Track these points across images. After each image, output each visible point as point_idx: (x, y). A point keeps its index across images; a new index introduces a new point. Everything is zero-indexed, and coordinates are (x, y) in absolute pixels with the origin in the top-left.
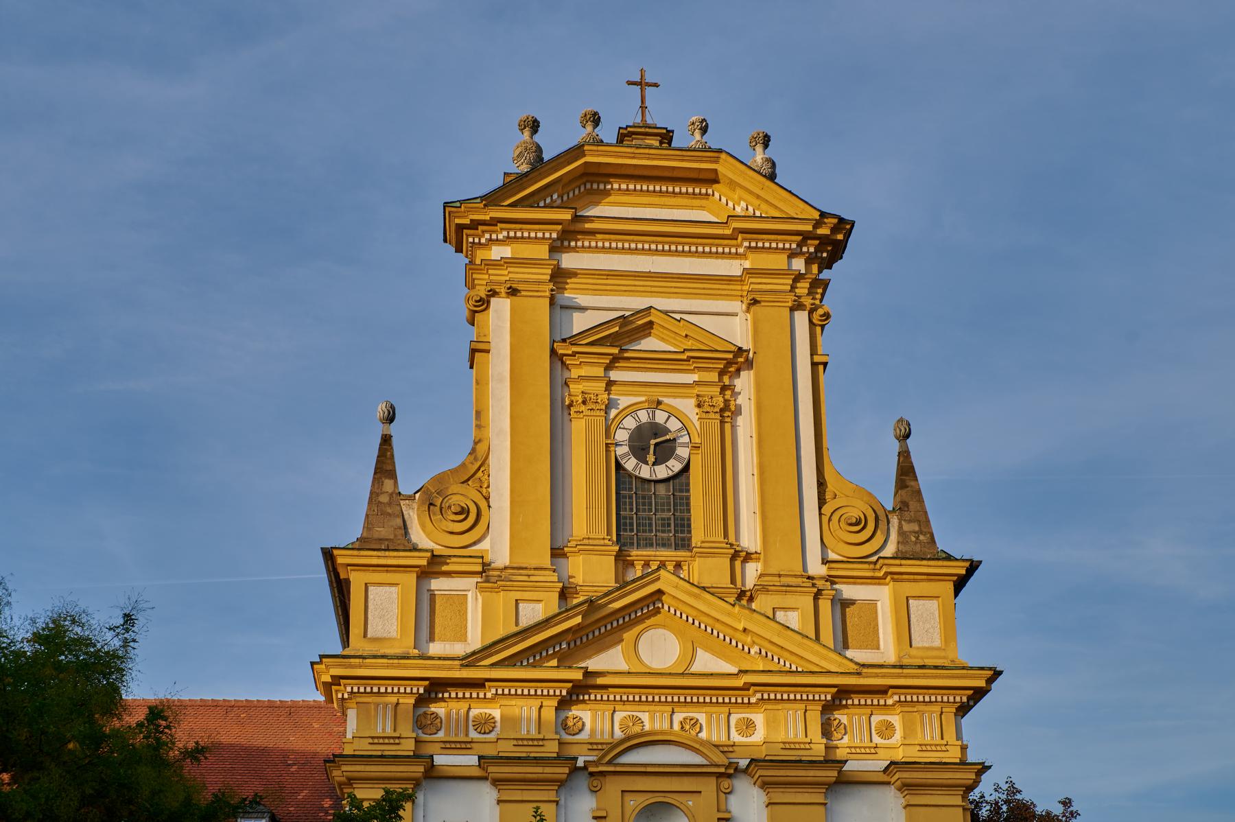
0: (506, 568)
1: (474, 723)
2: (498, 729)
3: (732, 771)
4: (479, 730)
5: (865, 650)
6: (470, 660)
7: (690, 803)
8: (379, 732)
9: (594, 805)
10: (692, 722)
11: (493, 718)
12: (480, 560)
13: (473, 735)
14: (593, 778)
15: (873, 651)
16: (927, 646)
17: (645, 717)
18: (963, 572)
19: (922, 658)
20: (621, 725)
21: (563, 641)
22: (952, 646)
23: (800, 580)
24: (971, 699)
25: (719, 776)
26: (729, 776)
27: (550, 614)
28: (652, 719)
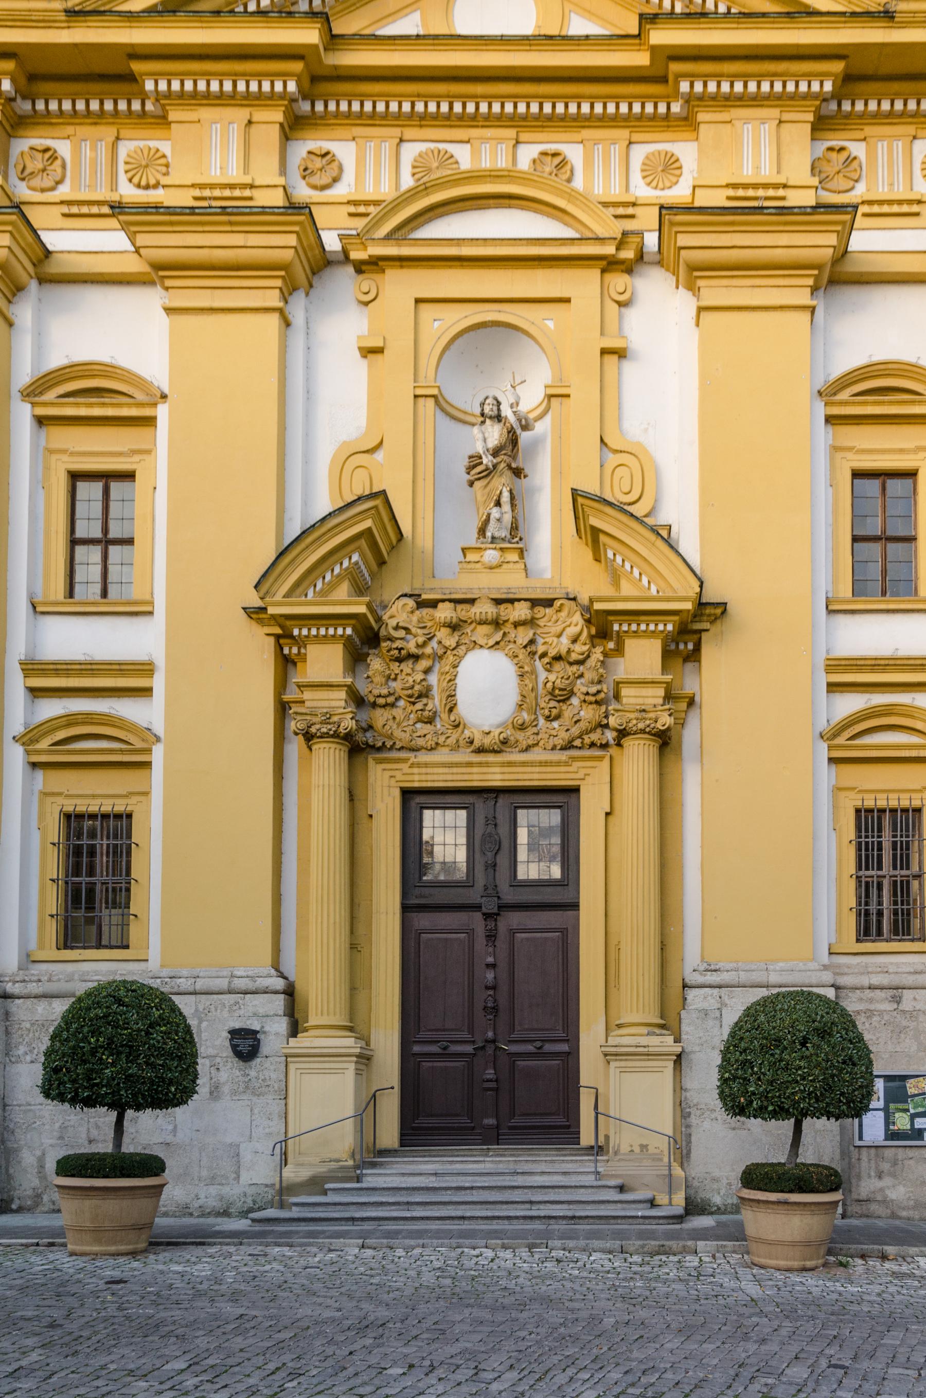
4: (136, 180)
10: (557, 160)
11: (164, 156)
28: (475, 154)
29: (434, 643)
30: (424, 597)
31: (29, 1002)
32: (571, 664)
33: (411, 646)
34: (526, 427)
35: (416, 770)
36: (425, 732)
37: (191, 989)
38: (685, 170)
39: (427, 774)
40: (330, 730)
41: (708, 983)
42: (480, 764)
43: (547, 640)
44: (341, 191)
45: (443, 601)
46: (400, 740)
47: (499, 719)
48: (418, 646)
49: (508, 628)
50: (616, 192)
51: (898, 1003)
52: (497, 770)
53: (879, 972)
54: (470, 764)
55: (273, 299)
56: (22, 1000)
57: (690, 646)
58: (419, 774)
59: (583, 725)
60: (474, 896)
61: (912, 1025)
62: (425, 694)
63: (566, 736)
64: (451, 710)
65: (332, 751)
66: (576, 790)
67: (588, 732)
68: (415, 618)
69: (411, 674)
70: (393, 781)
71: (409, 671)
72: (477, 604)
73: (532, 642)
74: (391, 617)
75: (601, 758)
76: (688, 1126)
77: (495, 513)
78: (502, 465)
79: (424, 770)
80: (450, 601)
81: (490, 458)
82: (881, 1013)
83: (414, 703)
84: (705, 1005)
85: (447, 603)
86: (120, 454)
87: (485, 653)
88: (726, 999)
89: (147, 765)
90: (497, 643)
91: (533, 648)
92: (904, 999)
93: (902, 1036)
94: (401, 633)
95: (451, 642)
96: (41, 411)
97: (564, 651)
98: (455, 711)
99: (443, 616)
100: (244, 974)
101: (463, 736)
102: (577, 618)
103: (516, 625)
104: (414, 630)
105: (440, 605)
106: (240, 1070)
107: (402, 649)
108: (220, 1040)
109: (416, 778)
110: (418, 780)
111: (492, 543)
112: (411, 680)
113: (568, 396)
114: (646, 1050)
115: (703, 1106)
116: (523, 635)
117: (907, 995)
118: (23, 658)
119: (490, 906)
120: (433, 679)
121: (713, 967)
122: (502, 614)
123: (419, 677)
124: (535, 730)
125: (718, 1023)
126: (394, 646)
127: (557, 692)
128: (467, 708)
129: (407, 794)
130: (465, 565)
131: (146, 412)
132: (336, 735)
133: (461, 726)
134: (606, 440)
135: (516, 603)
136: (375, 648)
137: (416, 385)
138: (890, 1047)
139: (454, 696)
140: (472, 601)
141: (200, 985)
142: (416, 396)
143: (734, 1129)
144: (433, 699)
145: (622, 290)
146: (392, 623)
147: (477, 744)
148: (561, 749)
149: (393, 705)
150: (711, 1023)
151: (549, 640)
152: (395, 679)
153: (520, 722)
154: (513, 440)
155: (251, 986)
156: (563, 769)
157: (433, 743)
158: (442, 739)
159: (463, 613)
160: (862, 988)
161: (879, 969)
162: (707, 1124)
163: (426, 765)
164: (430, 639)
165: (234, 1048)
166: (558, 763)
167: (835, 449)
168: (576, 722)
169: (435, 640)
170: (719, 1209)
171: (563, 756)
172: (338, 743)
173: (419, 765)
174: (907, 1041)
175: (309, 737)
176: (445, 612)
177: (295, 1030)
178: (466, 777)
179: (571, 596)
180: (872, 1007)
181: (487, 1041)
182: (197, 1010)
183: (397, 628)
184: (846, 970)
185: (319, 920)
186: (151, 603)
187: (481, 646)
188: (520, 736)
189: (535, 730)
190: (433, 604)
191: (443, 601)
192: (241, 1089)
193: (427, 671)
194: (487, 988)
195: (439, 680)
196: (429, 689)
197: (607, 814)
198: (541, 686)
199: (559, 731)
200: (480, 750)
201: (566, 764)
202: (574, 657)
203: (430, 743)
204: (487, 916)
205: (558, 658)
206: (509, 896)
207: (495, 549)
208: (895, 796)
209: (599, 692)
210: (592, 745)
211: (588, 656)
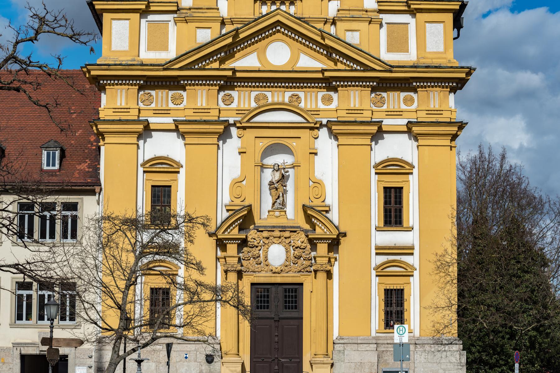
0: (190, 9)
1: (172, 99)
2: (185, 102)
3: (318, 125)
4: (174, 103)
5: (400, 53)
6: (168, 65)
7: (295, 144)
8: (118, 105)
9: (240, 145)
12: (176, 4)
13: (171, 106)
14: (239, 130)
15: (405, 53)
16: (435, 51)
17: (269, 94)
18: (458, 7)
19: (432, 59)
20: (255, 99)
21: (222, 51)
22: (450, 51)
23: (361, 13)
24: (459, 83)
25: (312, 129)
26: (318, 128)
27: (214, 38)
28: (273, 96)
29: (261, 242)
32: (301, 249)
33: (256, 244)
35: (255, 278)
38: (334, 100)
42: (274, 277)
43: (294, 242)
44: (234, 105)
47: (280, 264)
49: (283, 238)
50: (314, 107)
52: (279, 278)
55: (215, 141)
59: (304, 266)
63: (300, 269)
64: (266, 261)
66: (302, 284)
68: (256, 236)
69: (255, 251)
71: (255, 250)
73: (290, 242)
79: (258, 278)
91: (290, 244)
95: (267, 242)
97: (300, 246)
103: (286, 238)
104: (256, 239)
105: (264, 232)
109: (256, 280)
110: (256, 280)
116: (287, 241)
123: (258, 252)
128: (271, 260)
146: (250, 237)
147: (274, 271)
148: (298, 272)
149: (249, 260)
152: (250, 253)
153: (286, 265)
156: (298, 278)
158: (263, 269)
163: (259, 277)
166: (297, 277)
171: (298, 274)
173: (257, 277)
176: (265, 234)
178: (270, 280)
188: (286, 268)
193: (260, 250)
195: (263, 253)
196: (260, 255)
197: (311, 292)
198: (292, 254)
199: (298, 267)
200: (274, 273)
201: (299, 277)
202: (302, 247)
210: (307, 271)
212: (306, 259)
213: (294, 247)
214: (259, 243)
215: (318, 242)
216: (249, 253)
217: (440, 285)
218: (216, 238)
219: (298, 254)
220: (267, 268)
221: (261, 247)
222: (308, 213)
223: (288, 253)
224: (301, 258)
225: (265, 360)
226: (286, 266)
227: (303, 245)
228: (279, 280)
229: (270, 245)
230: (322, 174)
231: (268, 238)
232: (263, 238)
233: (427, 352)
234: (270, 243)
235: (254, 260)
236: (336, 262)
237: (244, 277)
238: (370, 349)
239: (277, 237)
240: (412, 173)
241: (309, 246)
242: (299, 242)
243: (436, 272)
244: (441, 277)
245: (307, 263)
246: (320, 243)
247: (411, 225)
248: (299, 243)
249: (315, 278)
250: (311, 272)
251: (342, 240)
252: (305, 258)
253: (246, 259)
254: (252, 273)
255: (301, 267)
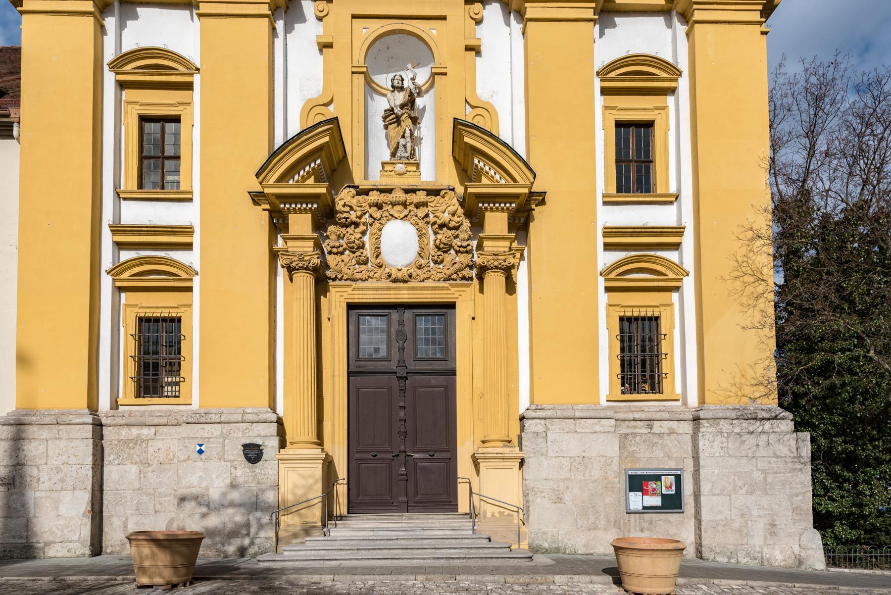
29: (367, 216)
30: (360, 187)
31: (116, 428)
32: (450, 229)
34: (419, 94)
35: (356, 292)
36: (362, 269)
37: (218, 420)
39: (362, 294)
40: (304, 265)
41: (538, 416)
45: (373, 190)
46: (346, 274)
47: (407, 262)
48: (357, 217)
49: (412, 207)
51: (651, 429)
53: (638, 411)
54: (389, 289)
56: (112, 427)
57: (522, 220)
58: (358, 294)
59: (457, 266)
60: (393, 366)
61: (660, 442)
62: (362, 247)
63: (448, 272)
64: (377, 257)
65: (305, 278)
67: (461, 270)
69: (353, 234)
70: (342, 299)
71: (352, 232)
72: (393, 192)
73: (427, 216)
74: (341, 200)
75: (468, 286)
76: (527, 501)
77: (402, 141)
78: (406, 115)
79: (361, 292)
80: (377, 190)
81: (399, 109)
82: (641, 434)
83: (354, 253)
84: (536, 429)
85: (375, 192)
86: (172, 105)
87: (399, 221)
88: (549, 426)
89: (190, 289)
90: (406, 216)
92: (655, 426)
93: (654, 448)
94: (347, 209)
95: (377, 215)
96: (121, 78)
98: (380, 257)
99: (373, 199)
100: (252, 411)
101: (385, 272)
102: (455, 201)
104: (355, 207)
105: (371, 193)
106: (250, 468)
107: (348, 218)
108: (237, 450)
109: (356, 297)
111: (400, 160)
112: (353, 237)
113: (445, 74)
114: (503, 455)
115: (536, 489)
116: (421, 212)
117: (656, 424)
118: (111, 223)
119: (402, 373)
120: (366, 239)
121: (539, 407)
122: (408, 198)
123: (359, 235)
124: (428, 269)
125: (545, 440)
126: (343, 216)
127: (442, 246)
128: (387, 255)
129: (351, 307)
130: (384, 173)
131: (187, 79)
132: (307, 269)
133: (384, 266)
134: (468, 100)
135: (417, 192)
136: (331, 219)
137: (353, 65)
138: (647, 455)
139: (379, 248)
140: (390, 191)
141: (223, 419)
142: (353, 73)
143: (555, 503)
144: (367, 250)
145: (477, 12)
147: (393, 276)
148: (444, 281)
149: (342, 253)
150: (540, 440)
151: (438, 214)
152: (343, 238)
153: (420, 264)
154: (410, 103)
155: (256, 418)
157: (367, 276)
158: (371, 274)
159: (385, 197)
160: (629, 420)
161: (638, 409)
162: (539, 500)
163: (363, 289)
164: (365, 214)
165: (246, 455)
166: (443, 288)
167: (606, 108)
168: (454, 264)
169: (368, 214)
170: (547, 550)
171: (447, 284)
172: (309, 273)
173: (358, 289)
174: (657, 451)
175: (290, 270)
176: (374, 197)
177: (283, 445)
179: (451, 188)
180: (635, 431)
181: (400, 452)
182: (222, 433)
183: (344, 206)
184: (618, 410)
185: (298, 379)
186: (191, 193)
187: (396, 218)
188: (419, 272)
189: (428, 269)
190: (366, 192)
191: (373, 190)
192: (250, 480)
193: (364, 233)
194: (400, 421)
195: (370, 238)
196: (363, 243)
198: (432, 242)
199: (445, 269)
200: (395, 281)
201: (448, 289)
202: (452, 224)
203: (364, 276)
204: (399, 378)
205: (441, 226)
206: (413, 366)
207: (402, 163)
208: (644, 309)
209: (468, 245)
210: (464, 278)
211: (462, 224)
212: (462, 249)
213: (436, 226)
214: (360, 217)
215: (486, 208)
216: (341, 240)
217: (744, 300)
218: (267, 207)
219: (443, 240)
220: (380, 272)
221: (365, 228)
222: (466, 143)
223: (424, 239)
224: (449, 250)
225: (379, 456)
226: (420, 267)
227: (456, 219)
228: (406, 296)
229: (384, 222)
230: (490, 93)
231: (379, 206)
232: (370, 207)
233: (726, 435)
234: (385, 218)
235: (352, 255)
236: (521, 263)
237: (333, 290)
238: (602, 429)
239: (399, 204)
240: (672, 91)
241: (467, 224)
242: (446, 214)
243: (735, 274)
244: (746, 285)
245: (463, 259)
246: (492, 210)
247: (673, 189)
248: (446, 217)
249: (481, 290)
250: (471, 279)
251: (537, 211)
252: (458, 249)
253: (335, 250)
254: (348, 282)
255: (451, 269)
